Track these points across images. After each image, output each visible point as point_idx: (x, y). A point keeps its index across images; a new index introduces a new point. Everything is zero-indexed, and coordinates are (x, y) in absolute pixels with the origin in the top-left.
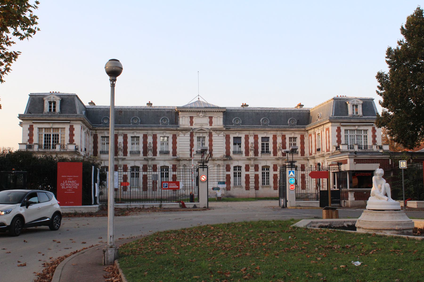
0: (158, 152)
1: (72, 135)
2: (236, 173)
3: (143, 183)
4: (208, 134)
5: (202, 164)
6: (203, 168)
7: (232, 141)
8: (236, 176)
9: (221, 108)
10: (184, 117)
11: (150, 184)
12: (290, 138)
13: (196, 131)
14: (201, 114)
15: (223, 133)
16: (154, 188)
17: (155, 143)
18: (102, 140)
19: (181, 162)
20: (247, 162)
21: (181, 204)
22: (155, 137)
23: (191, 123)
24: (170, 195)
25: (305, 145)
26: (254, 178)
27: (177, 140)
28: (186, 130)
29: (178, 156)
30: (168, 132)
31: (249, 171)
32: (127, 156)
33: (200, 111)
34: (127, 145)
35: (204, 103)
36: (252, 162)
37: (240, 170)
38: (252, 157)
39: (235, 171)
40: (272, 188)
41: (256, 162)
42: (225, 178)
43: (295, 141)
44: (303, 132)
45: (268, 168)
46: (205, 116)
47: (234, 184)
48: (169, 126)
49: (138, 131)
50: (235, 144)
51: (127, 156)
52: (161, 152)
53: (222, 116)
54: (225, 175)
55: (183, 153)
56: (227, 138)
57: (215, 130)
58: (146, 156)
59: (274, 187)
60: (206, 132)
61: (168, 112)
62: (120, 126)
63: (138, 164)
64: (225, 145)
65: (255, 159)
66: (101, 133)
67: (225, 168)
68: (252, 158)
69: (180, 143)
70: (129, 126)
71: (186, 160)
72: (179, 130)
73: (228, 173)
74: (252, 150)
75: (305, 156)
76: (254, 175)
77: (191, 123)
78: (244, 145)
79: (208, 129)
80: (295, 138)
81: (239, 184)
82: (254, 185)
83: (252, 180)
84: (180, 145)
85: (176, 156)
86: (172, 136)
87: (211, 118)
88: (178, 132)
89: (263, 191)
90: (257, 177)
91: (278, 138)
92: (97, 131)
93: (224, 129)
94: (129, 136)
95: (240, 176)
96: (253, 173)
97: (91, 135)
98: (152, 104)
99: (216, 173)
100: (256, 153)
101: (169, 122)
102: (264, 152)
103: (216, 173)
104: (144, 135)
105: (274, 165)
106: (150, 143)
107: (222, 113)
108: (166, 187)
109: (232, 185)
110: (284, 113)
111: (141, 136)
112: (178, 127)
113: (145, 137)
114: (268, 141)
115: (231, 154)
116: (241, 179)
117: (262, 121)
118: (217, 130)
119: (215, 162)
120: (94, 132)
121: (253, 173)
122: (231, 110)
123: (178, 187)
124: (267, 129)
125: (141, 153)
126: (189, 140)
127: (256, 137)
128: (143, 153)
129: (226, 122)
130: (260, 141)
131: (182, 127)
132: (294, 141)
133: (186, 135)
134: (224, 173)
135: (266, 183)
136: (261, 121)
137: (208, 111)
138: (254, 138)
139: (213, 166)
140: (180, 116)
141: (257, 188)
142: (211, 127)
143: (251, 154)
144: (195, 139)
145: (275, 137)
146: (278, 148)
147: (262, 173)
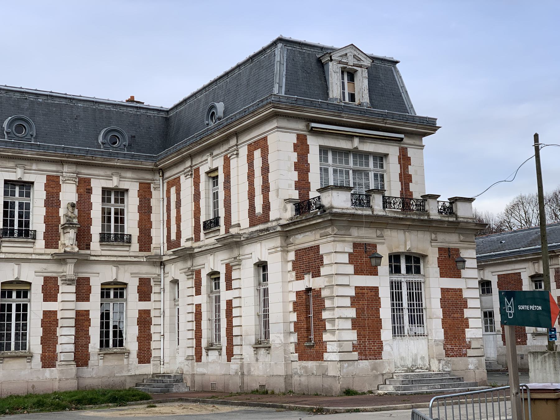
25: (153, 217)
40: (37, 359)
43: (122, 201)
44: (148, 176)
59: (43, 358)
75: (153, 252)
80: (121, 193)
91: (64, 187)
102: (12, 233)
105: (46, 279)
110: (85, 109)
132: (116, 201)
136: (5, 124)
145: (53, 186)
146: (63, 221)
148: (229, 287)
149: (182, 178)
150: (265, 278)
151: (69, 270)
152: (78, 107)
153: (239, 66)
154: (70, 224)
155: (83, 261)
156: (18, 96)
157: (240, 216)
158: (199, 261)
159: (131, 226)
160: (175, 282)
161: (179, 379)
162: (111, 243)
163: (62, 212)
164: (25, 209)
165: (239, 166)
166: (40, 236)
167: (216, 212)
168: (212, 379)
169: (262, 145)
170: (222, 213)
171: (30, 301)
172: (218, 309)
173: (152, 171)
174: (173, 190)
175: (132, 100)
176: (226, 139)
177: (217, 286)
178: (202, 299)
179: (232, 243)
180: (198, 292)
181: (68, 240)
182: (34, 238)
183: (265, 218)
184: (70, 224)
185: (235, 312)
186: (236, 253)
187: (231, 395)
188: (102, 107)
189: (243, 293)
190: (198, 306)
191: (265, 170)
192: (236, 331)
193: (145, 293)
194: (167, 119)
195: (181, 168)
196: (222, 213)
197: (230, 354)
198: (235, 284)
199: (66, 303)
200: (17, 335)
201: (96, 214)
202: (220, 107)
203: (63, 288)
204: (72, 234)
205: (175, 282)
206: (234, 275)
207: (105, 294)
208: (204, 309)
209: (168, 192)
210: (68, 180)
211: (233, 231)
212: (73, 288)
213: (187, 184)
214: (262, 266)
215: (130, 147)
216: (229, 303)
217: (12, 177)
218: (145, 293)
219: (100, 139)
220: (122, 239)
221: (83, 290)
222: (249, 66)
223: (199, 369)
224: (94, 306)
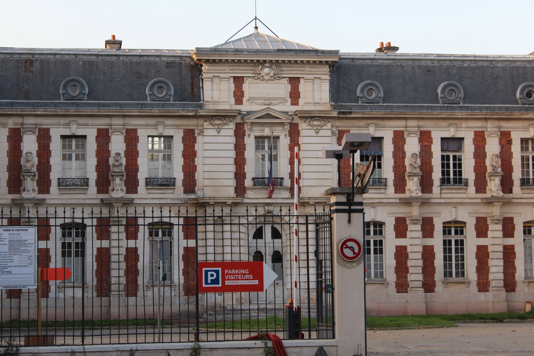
4: (287, 127)
5: (343, 199)
6: (350, 212)
9: (323, 52)
10: (216, 80)
11: (118, 274)
12: (524, 141)
13: (252, 119)
14: (266, 70)
15: (329, 125)
16: (132, 288)
17: (132, 153)
20: (402, 211)
21: (270, 344)
22: (131, 138)
23: (239, 96)
24: (175, 309)
26: (419, 256)
28: (224, 117)
29: (199, 193)
30: (169, 122)
31: (405, 236)
33: (265, 61)
34: (49, 162)
35: (273, 41)
36: (415, 211)
37: (381, 233)
38: (413, 195)
41: (427, 212)
46: (276, 77)
48: (173, 105)
49: (81, 121)
52: (149, 182)
53: (328, 77)
55: (215, 182)
57: (309, 117)
58: (107, 192)
59: (478, 284)
60: (283, 124)
61: (169, 65)
62: (28, 104)
68: (417, 198)
69: (207, 154)
70: (56, 105)
72: (202, 117)
74: (415, 175)
76: (420, 249)
78: (392, 160)
79: (287, 113)
81: (376, 274)
82: (420, 277)
83: (415, 262)
84: (207, 161)
85: (193, 192)
87: (294, 82)
88: (201, 121)
90: (428, 254)
91: (489, 140)
93: (335, 114)
94: (56, 134)
96: (418, 241)
98: (120, 43)
100: (426, 184)
101: (172, 93)
104: (99, 131)
105: (478, 219)
106: (118, 154)
107: (327, 69)
108: (216, 281)
110: (504, 69)
111: (91, 134)
112: (201, 106)
113: (103, 137)
114: (460, 149)
116: (381, 260)
117: (443, 91)
118: (312, 118)
121: (418, 241)
123: (256, 282)
124: (459, 114)
125: (92, 183)
126: (232, 147)
127: (425, 138)
128: (98, 183)
129: (338, 92)
130: (436, 149)
131: (211, 107)
133: (223, 132)
135: (455, 269)
136: (439, 90)
137: (287, 61)
138: (420, 141)
140: (204, 76)
141: (429, 286)
142: (295, 108)
143: (413, 186)
144: (250, 142)
145: (480, 139)
146: (489, 169)
147: (445, 241)
152: (498, 68)
156: (448, 62)
162: (531, 187)
166: (471, 183)
171: (465, 237)
182: (466, 185)
188: (519, 64)
200: (457, 265)
203: (491, 227)
210: (492, 134)
212: (500, 227)
219: (518, 95)
221: (508, 229)
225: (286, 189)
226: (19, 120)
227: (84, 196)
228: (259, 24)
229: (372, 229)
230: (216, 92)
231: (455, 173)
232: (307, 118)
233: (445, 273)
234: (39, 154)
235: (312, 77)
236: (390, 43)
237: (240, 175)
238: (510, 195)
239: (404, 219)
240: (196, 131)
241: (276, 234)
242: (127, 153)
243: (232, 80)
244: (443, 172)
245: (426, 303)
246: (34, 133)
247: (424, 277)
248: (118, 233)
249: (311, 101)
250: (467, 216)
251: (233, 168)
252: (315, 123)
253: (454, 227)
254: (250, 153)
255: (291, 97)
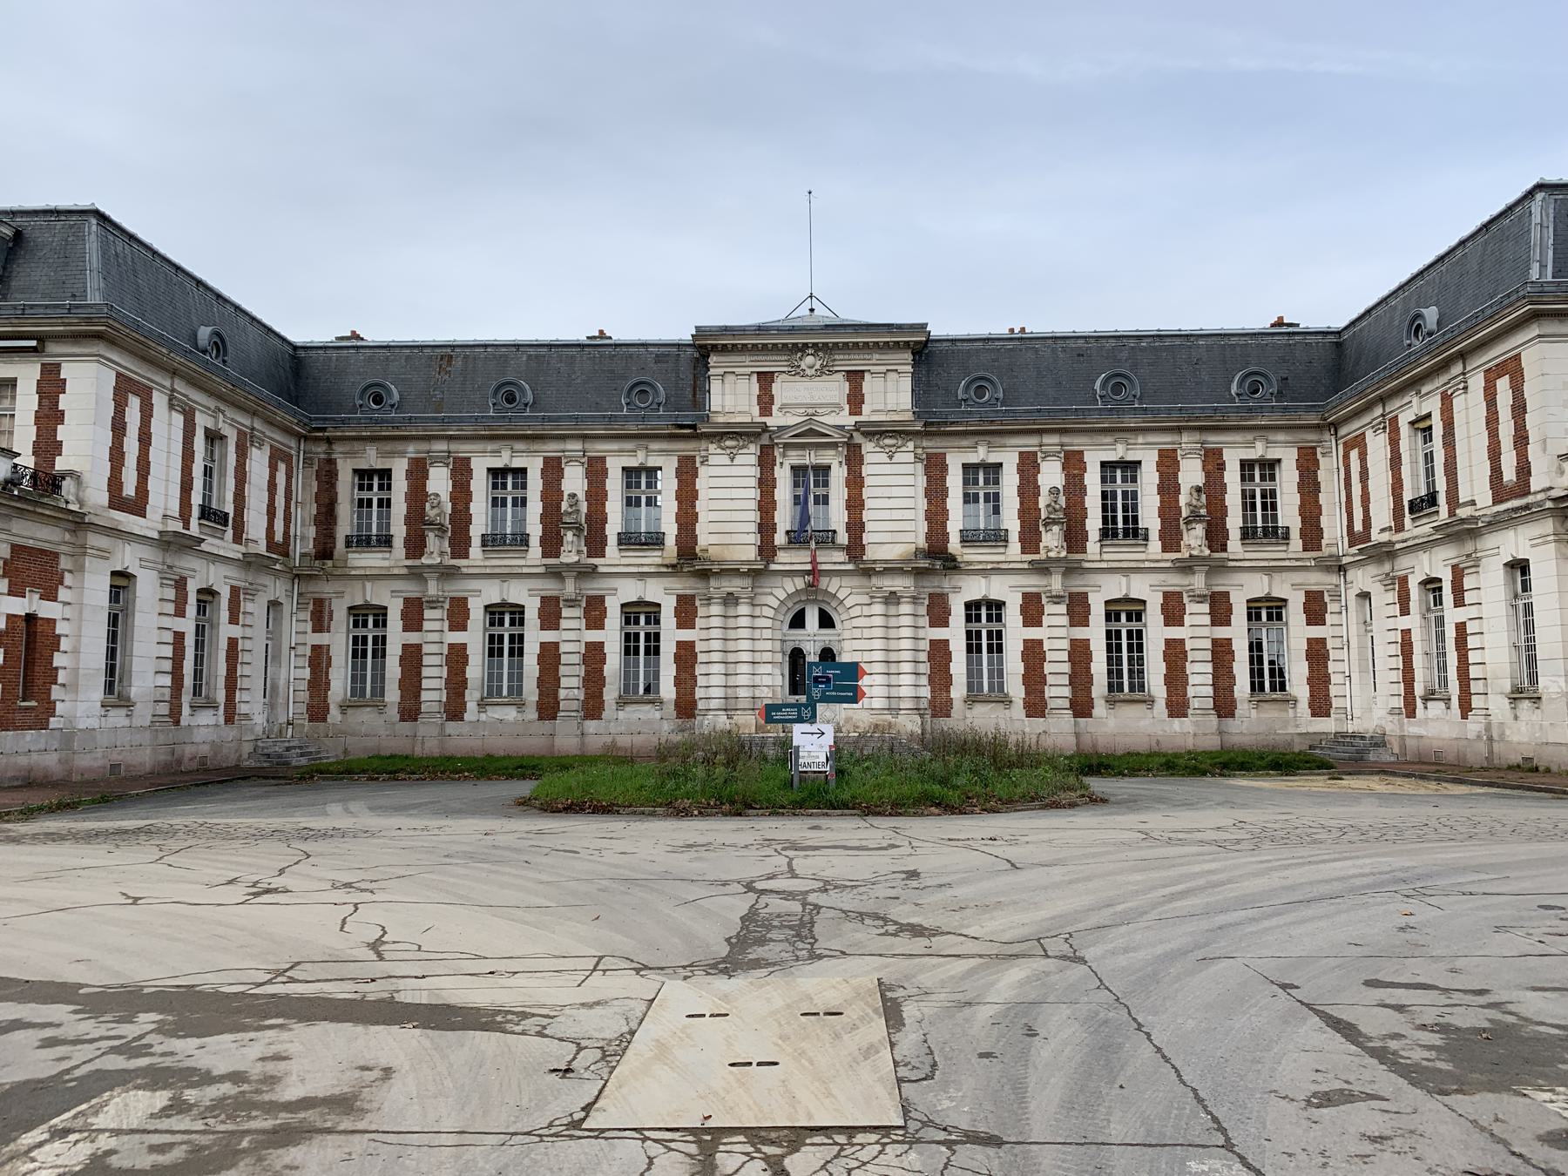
0: (612, 540)
1: (49, 416)
2: (979, 633)
3: (541, 682)
4: (843, 450)
7: (954, 481)
8: (979, 650)
10: (729, 378)
11: (571, 685)
12: (1246, 466)
14: (809, 360)
15: (911, 445)
16: (593, 707)
18: (361, 488)
19: (713, 583)
25: (1323, 499)
27: (701, 484)
28: (740, 434)
30: (654, 446)
32: (466, 556)
33: (806, 345)
36: (1056, 583)
37: (999, 618)
39: (974, 626)
42: (923, 657)
43: (1272, 478)
44: (1312, 436)
45: (1135, 609)
47: (970, 686)
49: (519, 446)
50: (969, 499)
51: (466, 556)
54: (925, 645)
56: (935, 469)
57: (876, 432)
59: (1169, 705)
61: (659, 358)
63: (517, 593)
64: (922, 504)
65: (1072, 570)
66: (351, 454)
67: (923, 610)
68: (1058, 560)
71: (736, 572)
73: (939, 633)
74: (1055, 522)
76: (1065, 644)
77: (766, 409)
79: (842, 427)
82: (1067, 692)
83: (1057, 666)
86: (676, 465)
87: (855, 378)
88: (703, 444)
89: (1117, 725)
91: (1184, 464)
92: (338, 448)
94: (480, 466)
95: (997, 648)
96: (1062, 632)
97: (308, 462)
99: (879, 632)
101: (662, 399)
102: (1115, 535)
103: (879, 632)
105: (1166, 595)
106: (574, 495)
107: (908, 356)
109: (958, 691)
110: (1209, 348)
112: (706, 419)
113: (553, 470)
115: (954, 545)
116: (1001, 662)
118: (882, 433)
119: (875, 581)
120: (321, 449)
121: (1062, 632)
122: (953, 341)
125: (535, 541)
126: (753, 482)
127: (1073, 464)
128: (544, 541)
131: (721, 419)
132: (1263, 478)
133: (739, 460)
134: (921, 633)
135: (1126, 681)
136: (1098, 385)
139: (865, 599)
140: (712, 371)
141: (1081, 707)
143: (1052, 540)
144: (783, 475)
145: (1168, 464)
147: (1109, 633)
148: (1459, 602)
149: (1369, 434)
150: (1526, 587)
151: (1198, 582)
152: (1198, 346)
153: (1462, 243)
154: (1195, 517)
155: (1218, 568)
157: (1475, 487)
158: (1403, 563)
159: (1289, 513)
160: (1365, 596)
161: (1379, 742)
163: (1183, 500)
164: (1131, 499)
165: (1470, 409)
166: (1154, 535)
167: (1431, 484)
168: (1436, 745)
169: (1512, 368)
170: (1441, 485)
172: (1441, 637)
173: (1318, 428)
174: (1354, 454)
175: (1280, 323)
176: (1444, 366)
177: (1438, 601)
178: (1413, 622)
179: (1463, 532)
180: (1405, 611)
181: (1194, 539)
182: (1146, 539)
183: (1522, 487)
184: (1195, 517)
185: (1472, 642)
186: (1469, 547)
187: (1471, 770)
188: (1234, 340)
189: (1485, 611)
190: (1406, 633)
191: (1519, 409)
192: (1474, 672)
193: (1315, 610)
194: (1338, 345)
195: (1366, 419)
196: (1441, 485)
197: (1466, 708)
198: (1469, 597)
199: (1196, 628)
200: (1131, 671)
201: (1233, 499)
202: (1431, 315)
203: (1191, 607)
204: (1199, 530)
205: (1365, 596)
206: (1468, 582)
207: (1253, 615)
208: (1416, 637)
209: (1346, 457)
211: (1462, 513)
212: (1206, 608)
213: (1377, 445)
214: (1519, 567)
215: (1280, 395)
216: (1461, 628)
217: (1111, 456)
218: (1315, 610)
219: (1234, 389)
220: (1275, 534)
221: (1220, 611)
222: (1480, 239)
223: (1412, 728)
224: (1238, 632)
225: (841, 548)
226: (424, 446)
227: (522, 562)
228: (816, 305)
229: (984, 612)
230: (730, 397)
231: (1126, 519)
232: (873, 434)
233: (1110, 686)
234: (453, 499)
235: (883, 369)
236: (1023, 330)
237: (766, 527)
238: (1224, 555)
239: (1038, 596)
240: (698, 460)
241: (826, 621)
242: (589, 495)
243: (755, 377)
244: (1105, 519)
245: (1077, 735)
246: (447, 465)
247: (1074, 692)
248: (572, 618)
249: (882, 407)
250: (1146, 589)
251: (754, 516)
252: (888, 441)
253: (1126, 610)
254: (784, 492)
255: (849, 402)
